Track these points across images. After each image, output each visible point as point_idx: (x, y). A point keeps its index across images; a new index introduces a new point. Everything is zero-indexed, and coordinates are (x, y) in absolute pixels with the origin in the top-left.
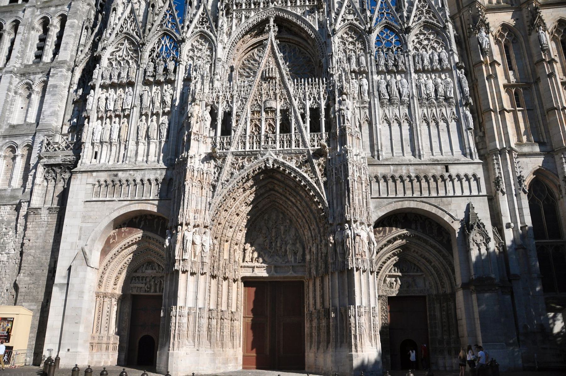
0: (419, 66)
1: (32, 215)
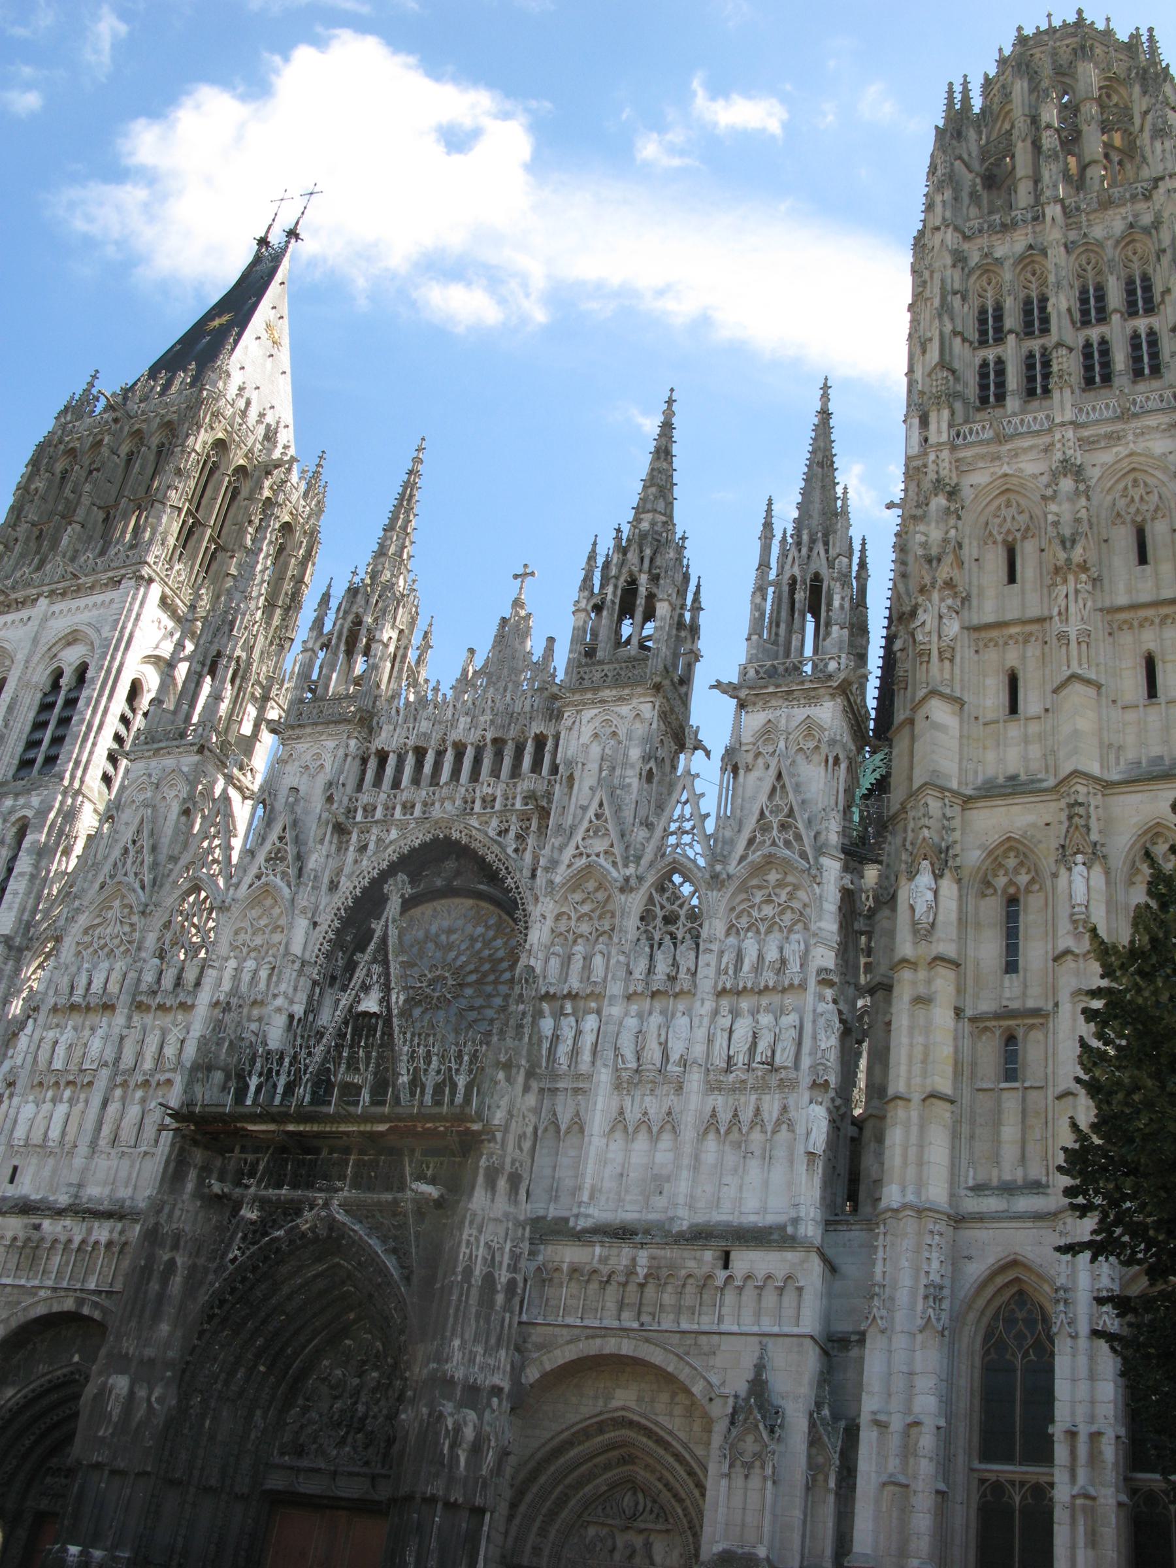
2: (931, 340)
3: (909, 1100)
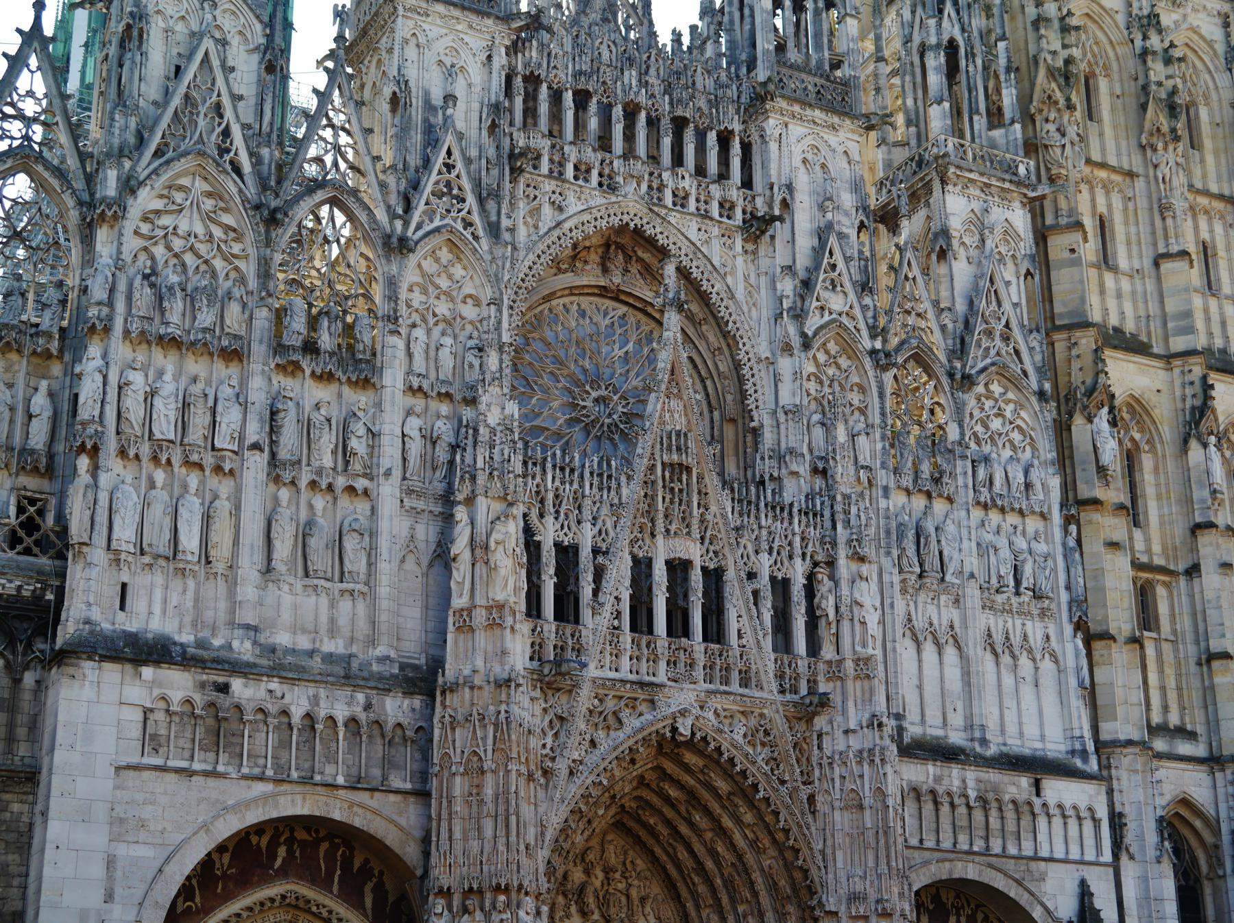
0: (985, 496)
3: (1113, 638)
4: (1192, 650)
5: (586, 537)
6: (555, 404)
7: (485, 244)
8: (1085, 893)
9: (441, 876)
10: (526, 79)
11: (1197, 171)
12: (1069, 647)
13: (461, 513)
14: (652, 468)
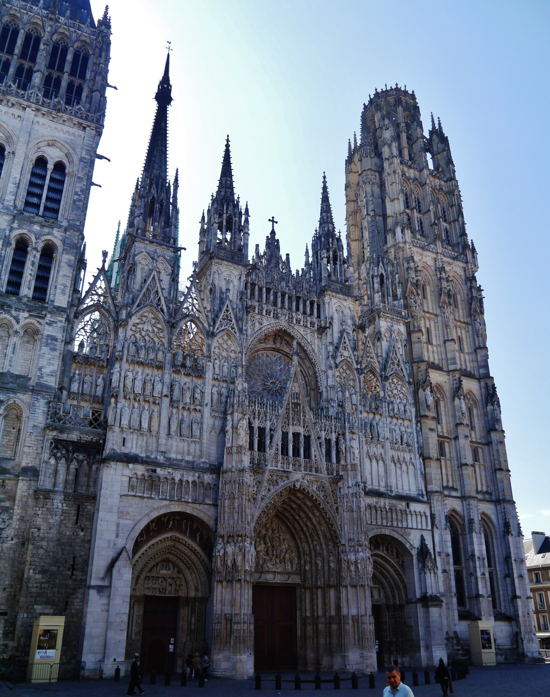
0: (392, 414)
1: (42, 500)
2: (398, 199)
3: (431, 459)
4: (456, 462)
5: (268, 425)
6: (259, 384)
7: (238, 334)
8: (423, 539)
9: (221, 531)
10: (251, 284)
11: (457, 315)
12: (418, 461)
13: (229, 417)
14: (288, 404)
